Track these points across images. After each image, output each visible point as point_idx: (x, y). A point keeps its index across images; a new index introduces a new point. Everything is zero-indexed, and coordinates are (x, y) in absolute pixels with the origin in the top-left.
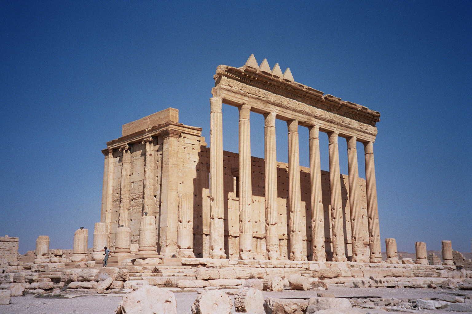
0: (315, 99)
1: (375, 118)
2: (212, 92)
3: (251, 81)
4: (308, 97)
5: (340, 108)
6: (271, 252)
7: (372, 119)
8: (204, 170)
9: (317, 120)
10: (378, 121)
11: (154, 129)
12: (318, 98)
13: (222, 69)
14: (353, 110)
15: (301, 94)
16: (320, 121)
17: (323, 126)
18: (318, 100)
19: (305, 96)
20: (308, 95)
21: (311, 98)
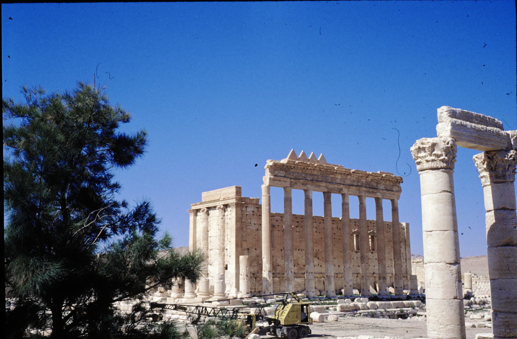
2: (263, 180)
7: (397, 181)
9: (347, 190)
10: (402, 182)
11: (224, 199)
13: (270, 163)
18: (348, 175)
20: (338, 172)
21: (342, 174)
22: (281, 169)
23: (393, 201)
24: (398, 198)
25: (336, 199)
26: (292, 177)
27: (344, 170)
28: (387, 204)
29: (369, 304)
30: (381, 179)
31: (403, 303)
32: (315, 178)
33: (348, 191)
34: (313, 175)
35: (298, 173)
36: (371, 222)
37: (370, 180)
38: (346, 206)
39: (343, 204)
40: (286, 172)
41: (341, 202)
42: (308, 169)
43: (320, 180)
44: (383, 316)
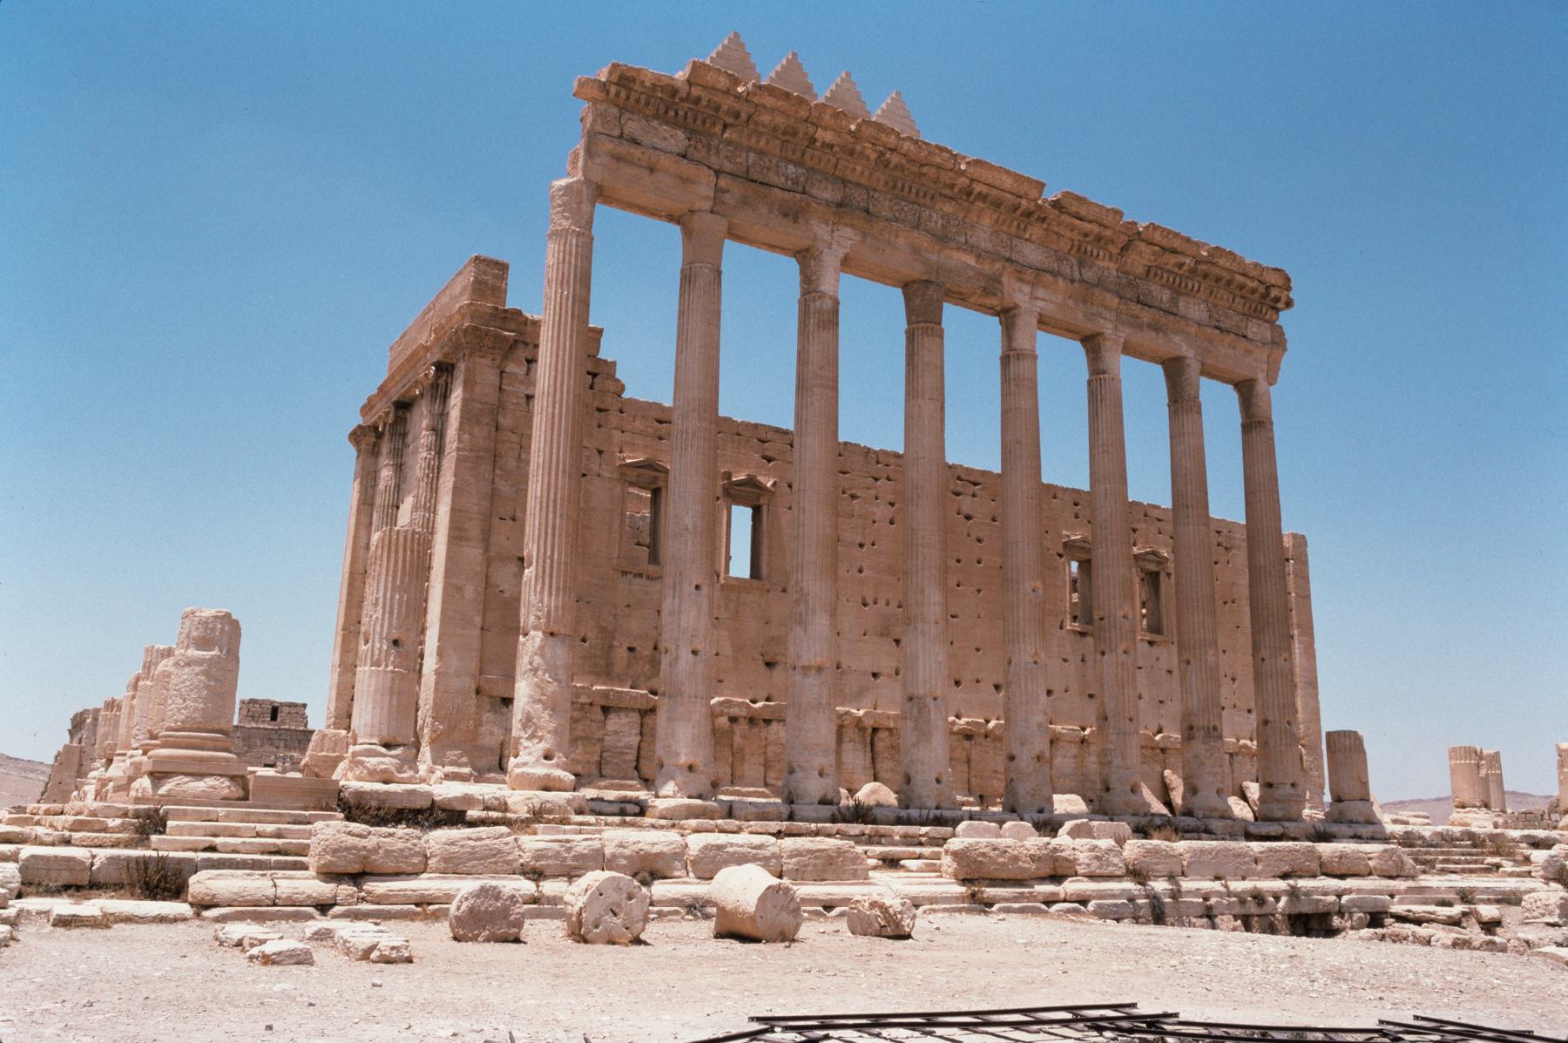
0: (1016, 208)
1: (1274, 293)
3: (725, 126)
4: (983, 197)
5: (1125, 249)
6: (799, 775)
8: (607, 474)
9: (1027, 289)
10: (1289, 304)
12: (1024, 202)
14: (1182, 259)
15: (952, 186)
16: (1041, 293)
17: (1050, 309)
18: (1029, 214)
19: (969, 194)
20: (978, 188)
21: (997, 204)
22: (662, 117)
23: (1246, 389)
24: (1272, 380)
25: (969, 337)
26: (728, 166)
27: (1008, 183)
28: (1218, 405)
29: (1134, 848)
30: (1193, 271)
31: (1312, 851)
32: (859, 197)
33: (1034, 298)
34: (845, 182)
35: (761, 153)
36: (1146, 512)
37: (1140, 270)
38: (1025, 365)
39: (1005, 360)
40: (691, 133)
41: (998, 352)
42: (813, 140)
44: (1209, 916)
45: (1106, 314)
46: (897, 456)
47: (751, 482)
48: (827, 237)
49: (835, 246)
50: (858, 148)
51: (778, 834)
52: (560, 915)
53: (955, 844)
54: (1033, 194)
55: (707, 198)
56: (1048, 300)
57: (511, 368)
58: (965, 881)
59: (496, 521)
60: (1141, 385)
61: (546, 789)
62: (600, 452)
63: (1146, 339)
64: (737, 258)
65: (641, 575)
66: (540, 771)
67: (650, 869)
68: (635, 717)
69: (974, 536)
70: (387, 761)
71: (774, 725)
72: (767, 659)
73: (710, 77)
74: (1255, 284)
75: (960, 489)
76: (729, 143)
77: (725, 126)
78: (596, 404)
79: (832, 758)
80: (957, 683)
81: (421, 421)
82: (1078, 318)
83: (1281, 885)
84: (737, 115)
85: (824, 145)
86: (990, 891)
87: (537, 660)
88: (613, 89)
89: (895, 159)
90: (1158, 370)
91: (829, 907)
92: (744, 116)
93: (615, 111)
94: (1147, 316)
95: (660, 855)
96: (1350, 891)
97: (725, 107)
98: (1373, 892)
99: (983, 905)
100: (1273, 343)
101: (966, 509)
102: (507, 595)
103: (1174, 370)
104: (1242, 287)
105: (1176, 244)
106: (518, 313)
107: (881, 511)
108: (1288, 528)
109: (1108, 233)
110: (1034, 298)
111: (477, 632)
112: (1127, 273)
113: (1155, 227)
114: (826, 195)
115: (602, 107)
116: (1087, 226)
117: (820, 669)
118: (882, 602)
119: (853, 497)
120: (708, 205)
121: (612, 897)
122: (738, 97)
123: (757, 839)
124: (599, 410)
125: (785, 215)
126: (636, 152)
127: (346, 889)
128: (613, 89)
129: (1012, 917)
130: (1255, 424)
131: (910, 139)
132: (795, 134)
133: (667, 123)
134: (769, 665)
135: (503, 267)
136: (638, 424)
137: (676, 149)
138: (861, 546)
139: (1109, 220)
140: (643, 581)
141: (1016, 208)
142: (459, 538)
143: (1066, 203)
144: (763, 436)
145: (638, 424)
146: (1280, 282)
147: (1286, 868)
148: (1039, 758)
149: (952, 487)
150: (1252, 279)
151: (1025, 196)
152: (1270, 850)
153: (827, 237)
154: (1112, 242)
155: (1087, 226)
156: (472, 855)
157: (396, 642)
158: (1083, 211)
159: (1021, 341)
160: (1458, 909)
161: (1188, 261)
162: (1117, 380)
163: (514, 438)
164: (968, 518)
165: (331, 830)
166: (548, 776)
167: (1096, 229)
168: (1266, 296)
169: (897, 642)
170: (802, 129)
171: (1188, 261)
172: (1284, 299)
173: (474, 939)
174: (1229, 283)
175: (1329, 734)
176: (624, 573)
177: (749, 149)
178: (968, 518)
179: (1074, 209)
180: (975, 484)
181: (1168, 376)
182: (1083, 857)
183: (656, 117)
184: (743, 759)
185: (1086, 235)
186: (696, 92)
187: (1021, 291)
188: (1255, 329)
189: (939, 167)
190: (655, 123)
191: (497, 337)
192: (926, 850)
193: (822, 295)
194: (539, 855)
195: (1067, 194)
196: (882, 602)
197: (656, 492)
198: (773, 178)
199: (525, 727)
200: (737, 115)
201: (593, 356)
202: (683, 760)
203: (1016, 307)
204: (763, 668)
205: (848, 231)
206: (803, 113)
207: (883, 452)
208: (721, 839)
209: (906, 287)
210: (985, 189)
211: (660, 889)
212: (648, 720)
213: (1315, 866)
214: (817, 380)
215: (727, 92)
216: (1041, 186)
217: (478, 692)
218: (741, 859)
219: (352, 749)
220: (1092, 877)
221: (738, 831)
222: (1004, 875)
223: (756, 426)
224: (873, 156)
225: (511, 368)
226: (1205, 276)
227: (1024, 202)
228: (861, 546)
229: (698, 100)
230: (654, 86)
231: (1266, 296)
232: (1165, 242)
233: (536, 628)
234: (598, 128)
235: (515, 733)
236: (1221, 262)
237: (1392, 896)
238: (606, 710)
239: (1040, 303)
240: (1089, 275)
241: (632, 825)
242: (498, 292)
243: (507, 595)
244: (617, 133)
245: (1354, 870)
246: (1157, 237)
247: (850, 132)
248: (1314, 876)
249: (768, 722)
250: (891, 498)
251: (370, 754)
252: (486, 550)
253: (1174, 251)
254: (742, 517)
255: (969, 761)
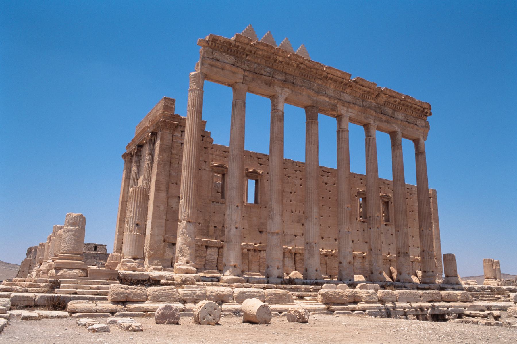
0: (342, 82)
1: (426, 110)
3: (247, 55)
4: (331, 79)
5: (377, 96)
6: (271, 269)
8: (207, 169)
9: (345, 109)
12: (344, 80)
14: (396, 99)
15: (321, 75)
16: (350, 110)
17: (353, 115)
18: (346, 84)
19: (327, 78)
20: (329, 76)
21: (336, 81)
23: (417, 142)
24: (425, 139)
25: (327, 124)
26: (248, 68)
27: (339, 74)
28: (408, 147)
29: (381, 292)
30: (399, 103)
31: (439, 293)
32: (290, 78)
33: (348, 112)
34: (286, 74)
35: (259, 64)
36: (384, 182)
37: (382, 103)
38: (345, 134)
39: (338, 132)
40: (236, 57)
41: (336, 130)
42: (276, 60)
43: (299, 84)
44: (405, 315)
45: (371, 117)
46: (303, 163)
47: (255, 172)
48: (280, 92)
49: (282, 95)
50: (291, 63)
51: (264, 288)
52: (192, 315)
53: (322, 291)
54: (348, 78)
55: (241, 79)
56: (353, 112)
57: (176, 134)
58: (325, 304)
59: (171, 184)
60: (383, 140)
61: (187, 273)
62: (205, 162)
63: (384, 125)
64: (250, 97)
65: (218, 202)
66: (185, 267)
67: (221, 300)
68: (216, 249)
69: (328, 189)
70: (134, 264)
71: (262, 252)
72: (260, 230)
73: (242, 39)
74: (419, 108)
75: (323, 174)
76: (248, 60)
77: (247, 55)
78: (204, 146)
79: (282, 262)
80: (322, 238)
81: (146, 151)
82: (362, 118)
83: (429, 304)
84: (251, 52)
85: (279, 61)
86: (334, 307)
87: (184, 230)
88: (210, 43)
89: (302, 66)
90: (388, 136)
91: (280, 312)
92: (253, 52)
93: (211, 50)
94: (384, 118)
95: (225, 295)
96: (451, 307)
97: (247, 49)
98: (459, 307)
99: (331, 312)
100: (425, 127)
101: (325, 181)
102: (174, 209)
103: (393, 135)
104: (415, 109)
105: (394, 94)
106: (178, 116)
107: (297, 182)
108: (431, 187)
109: (372, 91)
110: (348, 112)
111: (164, 221)
112: (378, 104)
113: (387, 89)
114: (280, 78)
115: (207, 49)
116: (365, 89)
117: (277, 234)
118: (298, 211)
119: (288, 177)
120: (241, 81)
121: (209, 309)
122: (251, 46)
123: (257, 290)
124: (205, 148)
125: (267, 84)
126: (218, 63)
127: (120, 307)
128: (210, 43)
129: (341, 316)
130: (419, 153)
131: (307, 60)
132: (270, 58)
133: (228, 54)
134: (261, 232)
135: (174, 101)
136: (218, 152)
137: (231, 63)
138: (291, 193)
139: (372, 87)
140: (219, 204)
141: (342, 82)
142: (159, 190)
143: (358, 81)
144: (259, 157)
145: (218, 152)
146: (427, 107)
147: (431, 299)
148: (349, 263)
149: (321, 174)
150: (419, 106)
151: (345, 78)
152: (425, 293)
153: (280, 92)
154: (373, 94)
155: (365, 89)
156: (163, 295)
157: (137, 225)
158: (364, 84)
159: (344, 126)
160: (486, 312)
161: (398, 100)
162: (374, 139)
163: (177, 157)
164: (326, 184)
165: (116, 287)
166: (187, 269)
167: (368, 89)
168: (423, 112)
169: (303, 224)
170: (272, 56)
171: (398, 100)
172: (429, 113)
173: (163, 323)
174: (411, 107)
175: (444, 255)
176: (213, 202)
177: (255, 63)
178: (326, 184)
179: (361, 83)
180: (328, 173)
181: (391, 137)
182: (364, 296)
183: (225, 52)
184: (252, 263)
185: (365, 91)
186: (237, 44)
187: (343, 109)
188: (419, 122)
189: (317, 69)
190: (224, 54)
191: (172, 124)
192: (313, 293)
193: (278, 111)
194: (185, 295)
195: (358, 78)
196: (298, 211)
197: (224, 175)
198: (262, 72)
199: (180, 253)
200: (251, 52)
201: (203, 130)
202: (232, 263)
203: (342, 115)
204: (259, 233)
205: (287, 90)
206: (273, 51)
207: (298, 162)
208: (245, 290)
209: (306, 108)
210: (332, 76)
211: (224, 306)
212: (221, 250)
213: (440, 298)
214: (277, 139)
215: (248, 44)
216: (350, 75)
217: (164, 241)
218: (251, 296)
219: (122, 260)
220: (367, 302)
221: (251, 287)
222: (338, 302)
223: (256, 153)
224: (295, 65)
225: (176, 134)
226: (403, 105)
227: (344, 80)
228: (291, 193)
229: (238, 47)
230: (224, 42)
231: (423, 112)
232: (390, 94)
233: (184, 220)
234: (205, 55)
235: (177, 255)
236: (409, 100)
237: (465, 308)
238: (207, 247)
239: (349, 113)
240: (365, 104)
241: (215, 285)
242: (172, 109)
243: (174, 209)
244: (211, 57)
245: (453, 300)
246: (388, 92)
247: (288, 57)
248: (440, 302)
249: (260, 251)
250: (301, 177)
251: (128, 261)
252: (167, 194)
253: (393, 97)
254: (252, 183)
255: (326, 264)
